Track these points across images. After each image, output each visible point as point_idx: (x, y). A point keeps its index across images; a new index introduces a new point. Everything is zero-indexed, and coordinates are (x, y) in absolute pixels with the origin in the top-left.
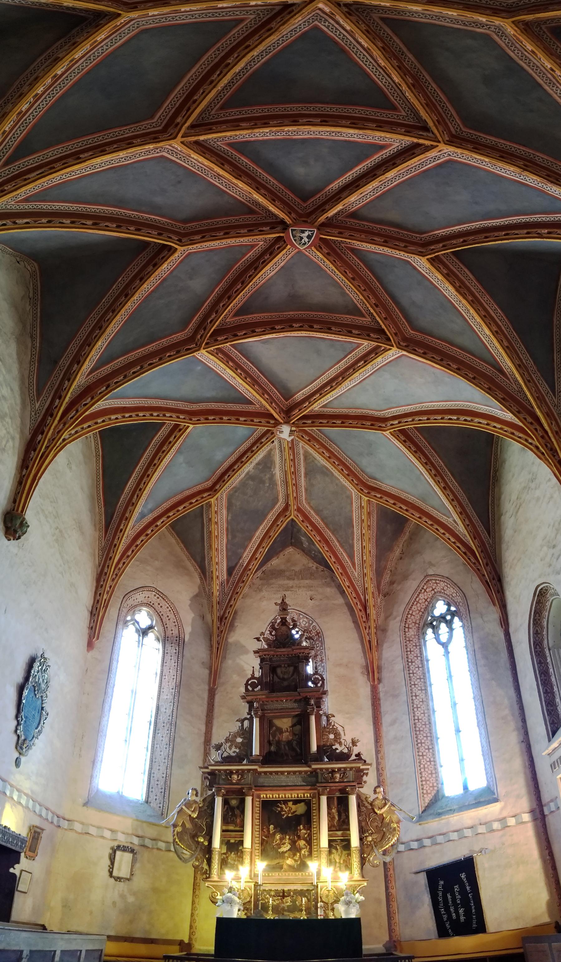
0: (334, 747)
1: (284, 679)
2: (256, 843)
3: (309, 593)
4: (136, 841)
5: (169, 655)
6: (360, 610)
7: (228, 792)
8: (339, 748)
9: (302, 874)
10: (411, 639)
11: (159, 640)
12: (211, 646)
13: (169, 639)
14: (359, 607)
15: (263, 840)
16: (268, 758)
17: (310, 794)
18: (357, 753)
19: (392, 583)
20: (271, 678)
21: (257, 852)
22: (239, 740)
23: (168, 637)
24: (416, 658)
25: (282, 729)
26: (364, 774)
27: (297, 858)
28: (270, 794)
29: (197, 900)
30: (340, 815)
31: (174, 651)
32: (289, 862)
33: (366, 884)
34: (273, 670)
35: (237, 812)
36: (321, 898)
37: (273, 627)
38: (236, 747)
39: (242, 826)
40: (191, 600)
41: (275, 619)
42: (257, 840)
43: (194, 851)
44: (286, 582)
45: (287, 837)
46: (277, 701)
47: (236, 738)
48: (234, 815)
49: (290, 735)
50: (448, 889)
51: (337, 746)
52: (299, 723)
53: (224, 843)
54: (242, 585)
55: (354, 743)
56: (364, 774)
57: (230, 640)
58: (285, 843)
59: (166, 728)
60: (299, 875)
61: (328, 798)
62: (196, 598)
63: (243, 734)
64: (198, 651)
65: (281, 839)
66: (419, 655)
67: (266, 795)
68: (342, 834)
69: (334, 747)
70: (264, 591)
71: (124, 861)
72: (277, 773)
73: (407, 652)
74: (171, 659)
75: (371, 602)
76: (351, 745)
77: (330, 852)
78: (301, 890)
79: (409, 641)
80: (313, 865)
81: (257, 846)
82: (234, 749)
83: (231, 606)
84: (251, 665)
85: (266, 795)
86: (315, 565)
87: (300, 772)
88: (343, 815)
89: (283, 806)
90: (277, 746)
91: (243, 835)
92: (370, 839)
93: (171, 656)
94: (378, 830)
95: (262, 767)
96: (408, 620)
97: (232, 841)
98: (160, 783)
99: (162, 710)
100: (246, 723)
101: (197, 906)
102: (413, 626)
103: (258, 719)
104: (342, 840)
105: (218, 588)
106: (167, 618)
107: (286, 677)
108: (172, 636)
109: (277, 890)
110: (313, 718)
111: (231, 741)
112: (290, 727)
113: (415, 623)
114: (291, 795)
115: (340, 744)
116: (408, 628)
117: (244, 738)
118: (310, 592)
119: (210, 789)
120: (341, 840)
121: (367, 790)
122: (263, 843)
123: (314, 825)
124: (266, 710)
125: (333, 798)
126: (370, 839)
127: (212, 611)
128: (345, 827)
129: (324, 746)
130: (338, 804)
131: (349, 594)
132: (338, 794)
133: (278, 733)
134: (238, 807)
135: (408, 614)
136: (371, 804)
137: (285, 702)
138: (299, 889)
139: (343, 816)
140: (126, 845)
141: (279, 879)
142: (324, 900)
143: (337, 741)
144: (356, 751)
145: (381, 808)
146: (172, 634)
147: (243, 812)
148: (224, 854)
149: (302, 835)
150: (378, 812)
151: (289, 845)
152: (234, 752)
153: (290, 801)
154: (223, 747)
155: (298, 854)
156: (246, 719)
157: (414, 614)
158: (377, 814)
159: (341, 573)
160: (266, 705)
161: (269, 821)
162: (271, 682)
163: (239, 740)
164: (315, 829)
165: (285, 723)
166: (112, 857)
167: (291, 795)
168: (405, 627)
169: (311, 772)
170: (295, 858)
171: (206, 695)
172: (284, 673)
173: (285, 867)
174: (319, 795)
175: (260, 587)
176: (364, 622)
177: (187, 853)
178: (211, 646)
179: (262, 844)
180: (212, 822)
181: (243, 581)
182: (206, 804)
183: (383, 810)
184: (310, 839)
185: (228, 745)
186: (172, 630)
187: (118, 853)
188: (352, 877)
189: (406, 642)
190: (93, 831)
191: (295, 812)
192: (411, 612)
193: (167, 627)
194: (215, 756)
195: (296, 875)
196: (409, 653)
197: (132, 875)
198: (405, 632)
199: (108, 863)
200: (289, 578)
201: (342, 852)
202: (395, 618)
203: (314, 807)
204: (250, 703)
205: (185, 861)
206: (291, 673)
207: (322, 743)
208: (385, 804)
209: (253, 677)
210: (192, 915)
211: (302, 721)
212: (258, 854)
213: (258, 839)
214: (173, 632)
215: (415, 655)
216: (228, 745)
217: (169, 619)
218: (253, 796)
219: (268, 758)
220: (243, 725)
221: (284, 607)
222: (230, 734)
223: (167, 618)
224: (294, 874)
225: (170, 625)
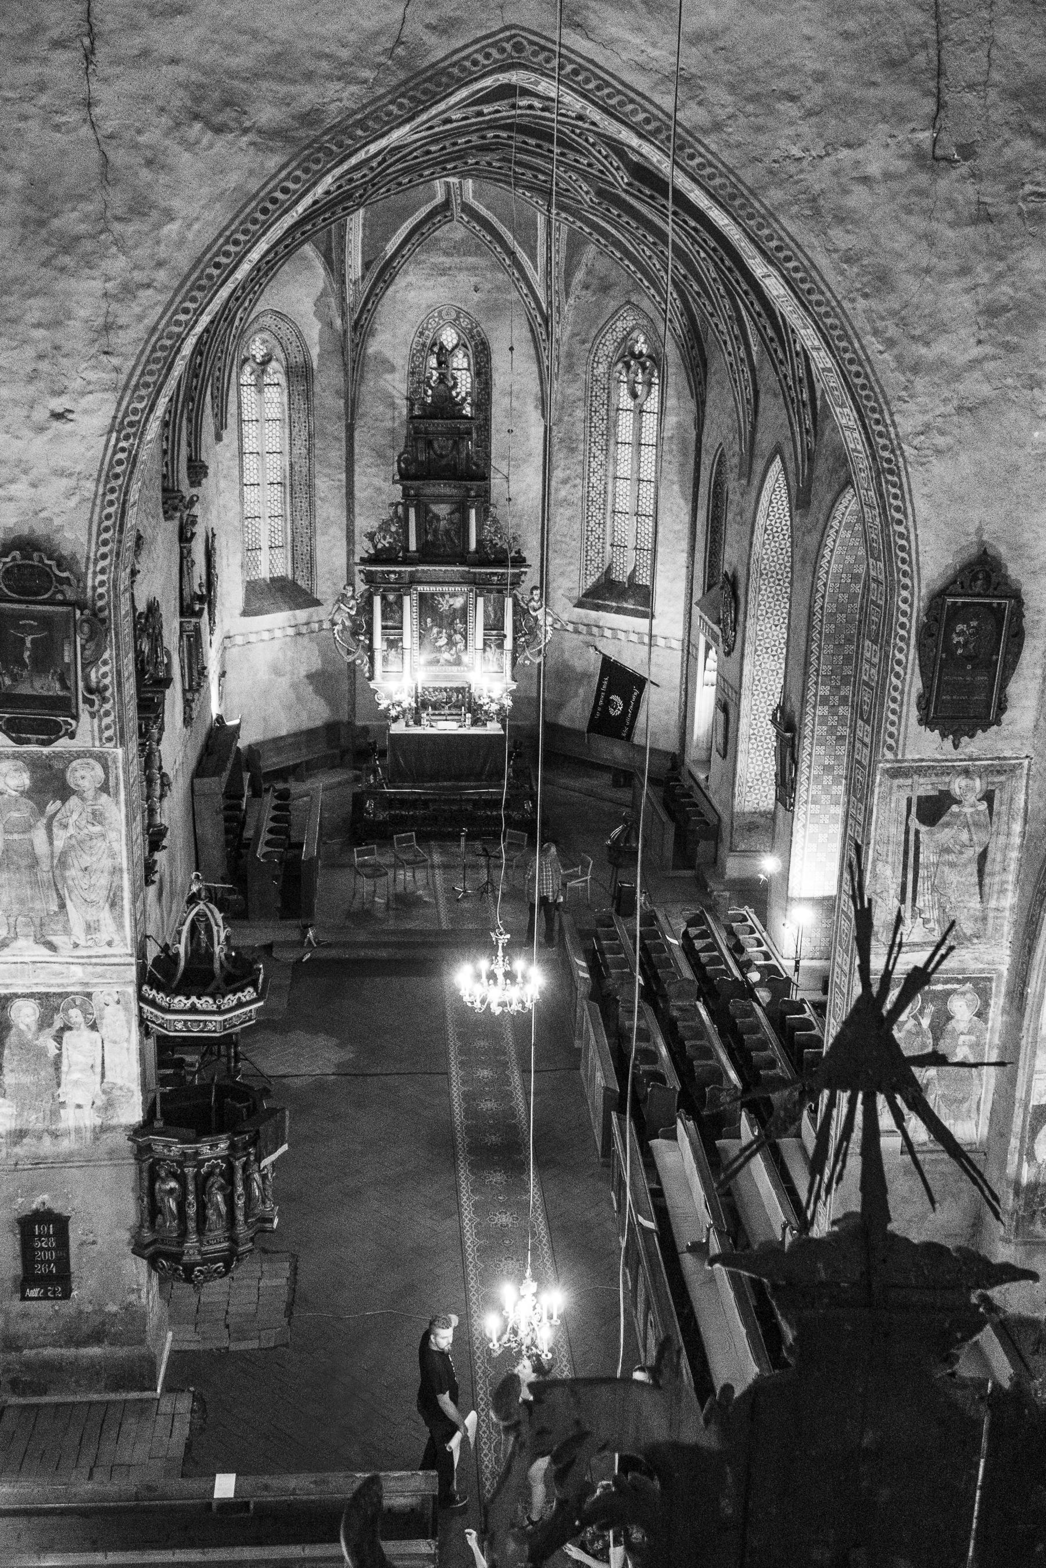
12: (345, 365)
27: (453, 652)
32: (446, 656)
51: (496, 540)
57: (370, 351)
77: (484, 650)
81: (416, 640)
122: (421, 637)
147: (401, 608)
156: (399, 503)
172: (442, 448)
173: (442, 661)
178: (345, 365)
180: (372, 619)
190: (253, 638)
211: (462, 510)
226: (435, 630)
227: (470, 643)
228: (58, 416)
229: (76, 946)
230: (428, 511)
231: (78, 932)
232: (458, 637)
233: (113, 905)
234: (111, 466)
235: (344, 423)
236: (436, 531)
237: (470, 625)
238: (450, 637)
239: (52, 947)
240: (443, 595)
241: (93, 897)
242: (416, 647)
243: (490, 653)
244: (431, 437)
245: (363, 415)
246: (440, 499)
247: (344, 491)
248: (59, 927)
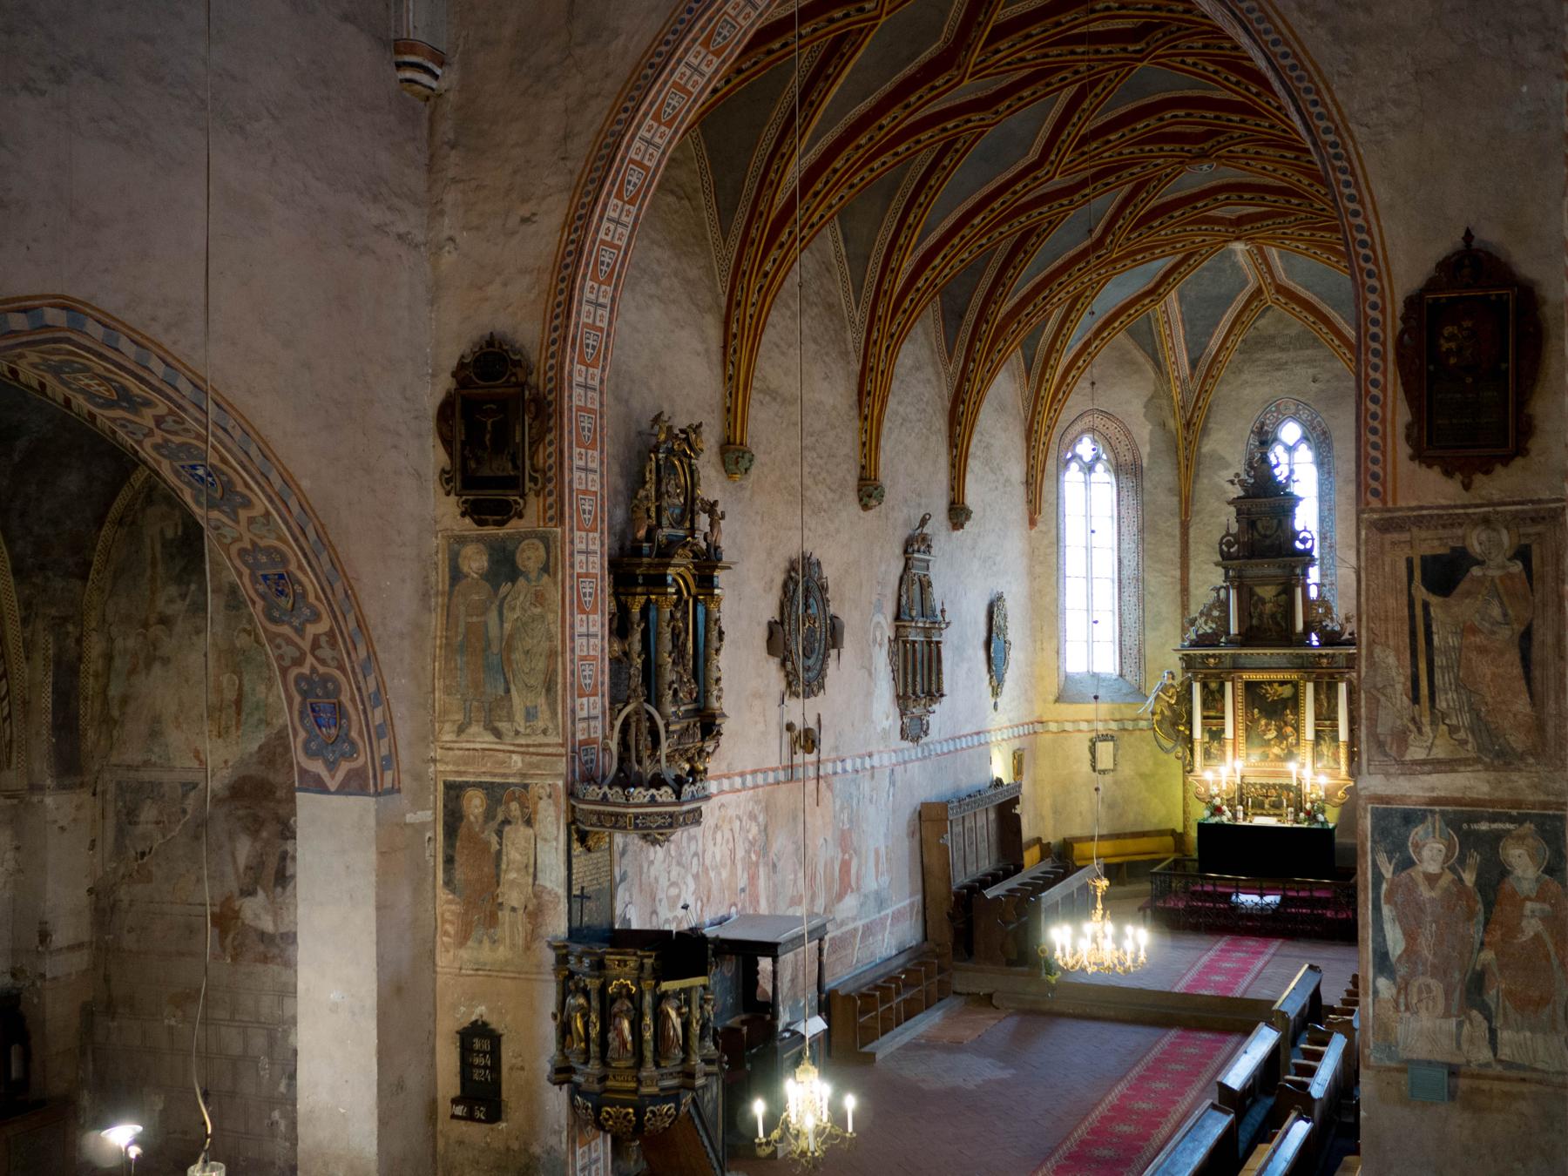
35: (1217, 696)
37: (1250, 465)
48: (1213, 700)
51: (1327, 622)
57: (1205, 449)
64: (1162, 475)
71: (1105, 750)
81: (1241, 733)
84: (1227, 518)
99: (1125, 562)
110: (1299, 591)
137: (1268, 568)
163: (1216, 613)
165: (1267, 592)
171: (1177, 532)
205: (1167, 751)
218: (1233, 680)
219: (1250, 637)
226: (1263, 722)
228: (524, 220)
229: (517, 733)
230: (1252, 593)
231: (519, 717)
233: (548, 690)
234: (563, 258)
235: (1177, 520)
236: (1261, 615)
239: (498, 734)
240: (1270, 683)
241: (532, 682)
242: (1242, 740)
244: (1254, 517)
246: (1264, 581)
247: (1178, 587)
248: (504, 713)
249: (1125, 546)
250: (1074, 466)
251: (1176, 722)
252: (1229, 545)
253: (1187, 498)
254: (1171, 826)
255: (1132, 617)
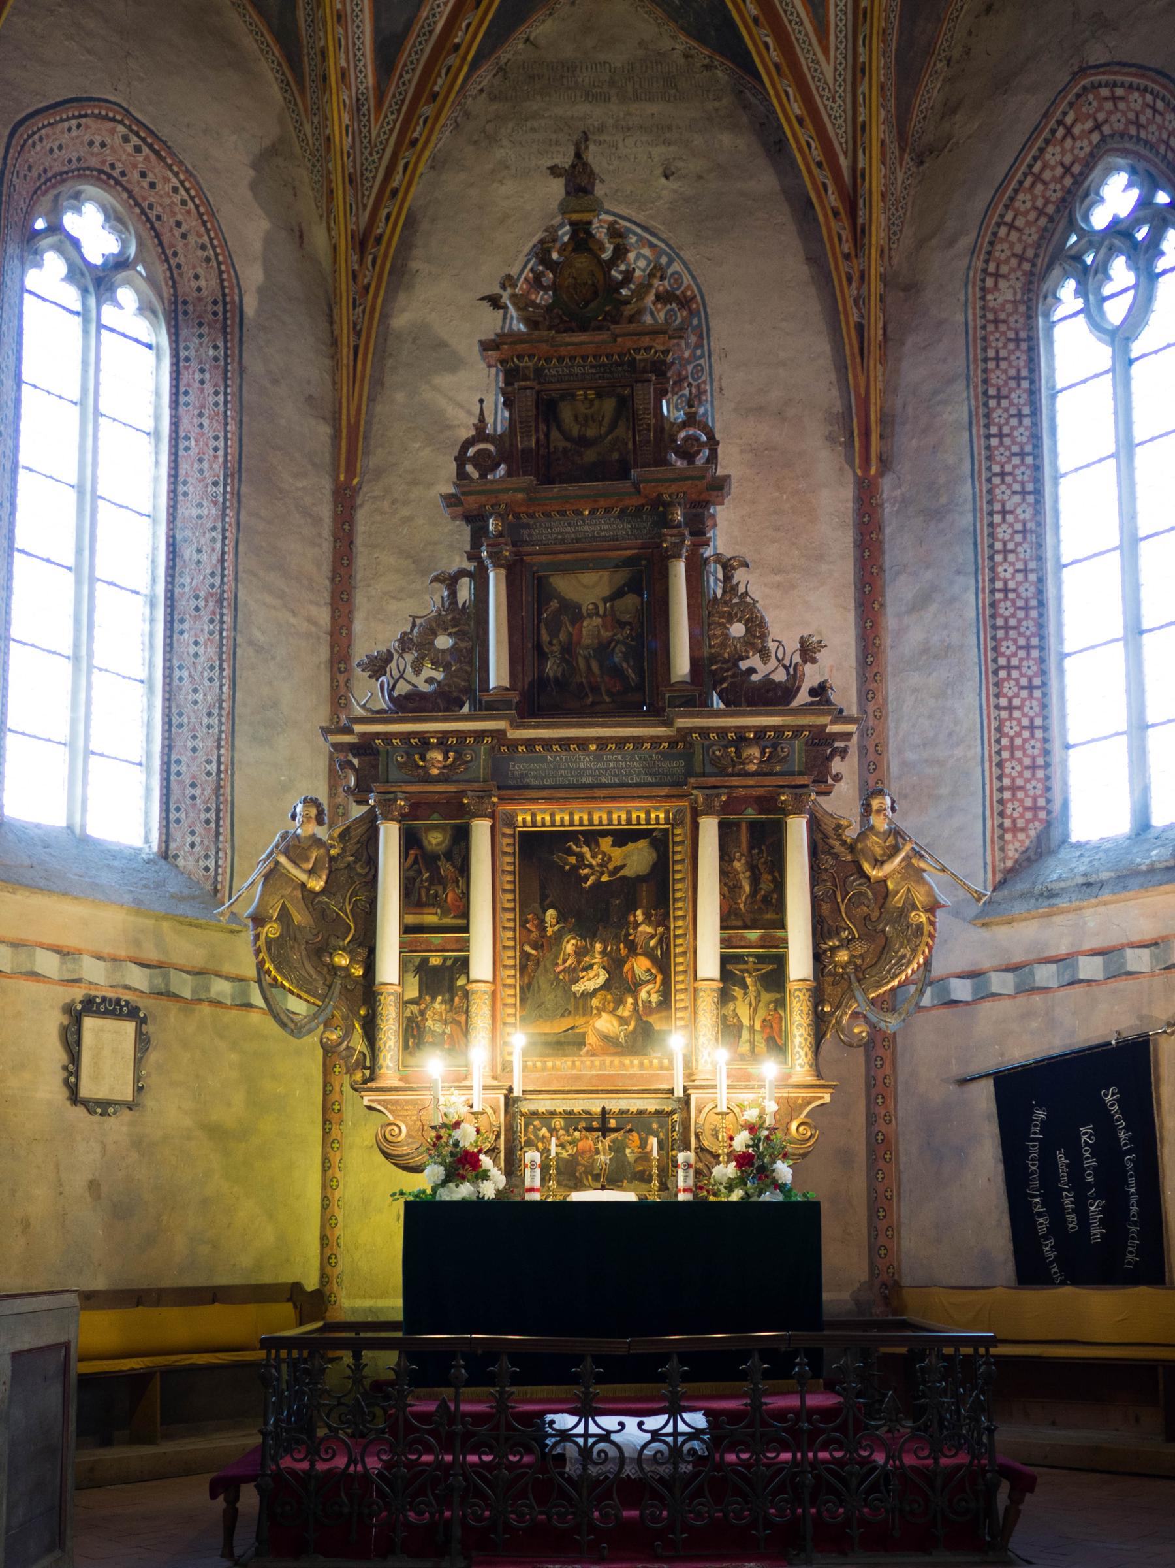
0: (744, 665)
1: (583, 442)
2: (505, 967)
3: (659, 151)
4: (138, 978)
5: (194, 364)
6: (836, 214)
7: (418, 808)
8: (760, 668)
9: (641, 1064)
10: (1003, 316)
11: (154, 312)
13: (190, 308)
14: (833, 199)
15: (526, 956)
16: (538, 697)
17: (667, 812)
18: (816, 684)
19: (950, 109)
20: (542, 437)
21: (510, 996)
22: (444, 642)
23: (185, 303)
24: (1012, 384)
25: (579, 607)
26: (835, 751)
27: (626, 1011)
28: (544, 811)
29: (335, 1157)
30: (755, 881)
31: (211, 352)
32: (605, 1023)
33: (827, 1098)
34: (547, 409)
35: (446, 869)
36: (697, 1136)
37: (542, 253)
38: (436, 664)
39: (465, 914)
40: (255, 166)
41: (552, 231)
42: (509, 958)
43: (322, 998)
44: (583, 108)
45: (598, 947)
46: (562, 513)
47: (436, 636)
48: (436, 880)
49: (604, 625)
50: (1060, 1134)
52: (634, 586)
53: (411, 967)
54: (428, 110)
55: (808, 651)
56: (835, 751)
58: (591, 966)
59: (203, 613)
60: (632, 1065)
61: (721, 825)
62: (267, 158)
63: (455, 622)
65: (580, 953)
66: (1024, 373)
67: (533, 815)
68: (762, 938)
69: (744, 665)
70: (505, 142)
72: (564, 743)
73: (985, 360)
74: (202, 382)
75: (876, 180)
76: (797, 659)
77: (725, 996)
78: (641, 1112)
79: (996, 322)
80: (676, 1040)
81: (509, 976)
82: (428, 671)
83: (395, 192)
84: (470, 397)
85: (533, 815)
86: (683, 42)
87: (638, 741)
88: (766, 877)
89: (585, 849)
90: (563, 659)
91: (468, 941)
92: (843, 956)
93: (202, 371)
94: (870, 931)
95: (516, 726)
96: (998, 247)
97: (435, 961)
98: (197, 788)
100: (465, 592)
101: (338, 1175)
102: (1012, 270)
103: (503, 572)
104: (760, 959)
105: (346, 120)
106: (177, 233)
107: (591, 433)
108: (200, 299)
109: (571, 1113)
111: (419, 646)
112: (605, 600)
113: (1021, 258)
114: (610, 814)
115: (764, 654)
116: (997, 275)
117: (459, 635)
118: (662, 149)
119: (361, 797)
120: (756, 956)
121: (841, 801)
122: (525, 965)
123: (679, 908)
124: (527, 543)
125: (737, 824)
126: (843, 956)
127: (329, 212)
128: (769, 916)
129: (713, 659)
130: (751, 848)
131: (800, 149)
132: (751, 814)
133: (565, 619)
134: (449, 855)
135: (998, 225)
136: (852, 848)
138: (634, 1109)
139: (766, 885)
140: (111, 994)
141: (577, 1078)
142: (706, 1143)
143: (752, 645)
144: (811, 676)
145: (882, 863)
146: (199, 289)
147: (464, 869)
148: (412, 1002)
149: (640, 940)
150: (874, 873)
151: (602, 972)
152: (430, 680)
153: (604, 834)
154: (393, 665)
155: (630, 1000)
157: (1020, 222)
158: (868, 878)
159: (777, 66)
160: (527, 526)
161: (544, 897)
162: (542, 451)
163: (444, 642)
164: (680, 923)
165: (587, 589)
166: (72, 1038)
167: (610, 814)
168: (984, 271)
169: (673, 743)
170: (620, 1012)
173: (591, 1039)
174: (696, 814)
175: (490, 128)
176: (847, 257)
177: (297, 1006)
179: (523, 968)
180: (373, 902)
181: (434, 96)
182: (352, 846)
183: (888, 868)
184: (666, 953)
185: (409, 657)
186: (197, 277)
187: (89, 1022)
188: (789, 1076)
189: (984, 327)
191: (622, 867)
192: (1008, 218)
193: (179, 266)
194: (368, 694)
195: (622, 1064)
196: (991, 365)
197: (139, 1090)
198: (983, 289)
199: (61, 1056)
200: (590, 96)
201: (759, 994)
202: (952, 242)
203: (679, 852)
204: (476, 521)
206: (607, 421)
207: (706, 652)
208: (896, 850)
209: (481, 434)
210: (326, 1203)
212: (511, 1001)
213: (511, 953)
214: (202, 283)
215: (1012, 372)
216: (409, 657)
217: (184, 236)
218: (492, 816)
219: (538, 697)
220: (453, 594)
221: (579, 181)
222: (414, 625)
223: (177, 233)
224: (617, 1060)
225: (190, 257)
227: (679, 981)
230: (543, 592)
232: (640, 965)
236: (568, 650)
237: (678, 926)
238: (615, 966)
240: (591, 837)
243: (742, 1009)
245: (379, 473)
249: (188, 510)
250: (53, 265)
251: (320, 942)
252: (485, 463)
253: (353, 430)
254: (288, 1277)
255: (201, 696)
